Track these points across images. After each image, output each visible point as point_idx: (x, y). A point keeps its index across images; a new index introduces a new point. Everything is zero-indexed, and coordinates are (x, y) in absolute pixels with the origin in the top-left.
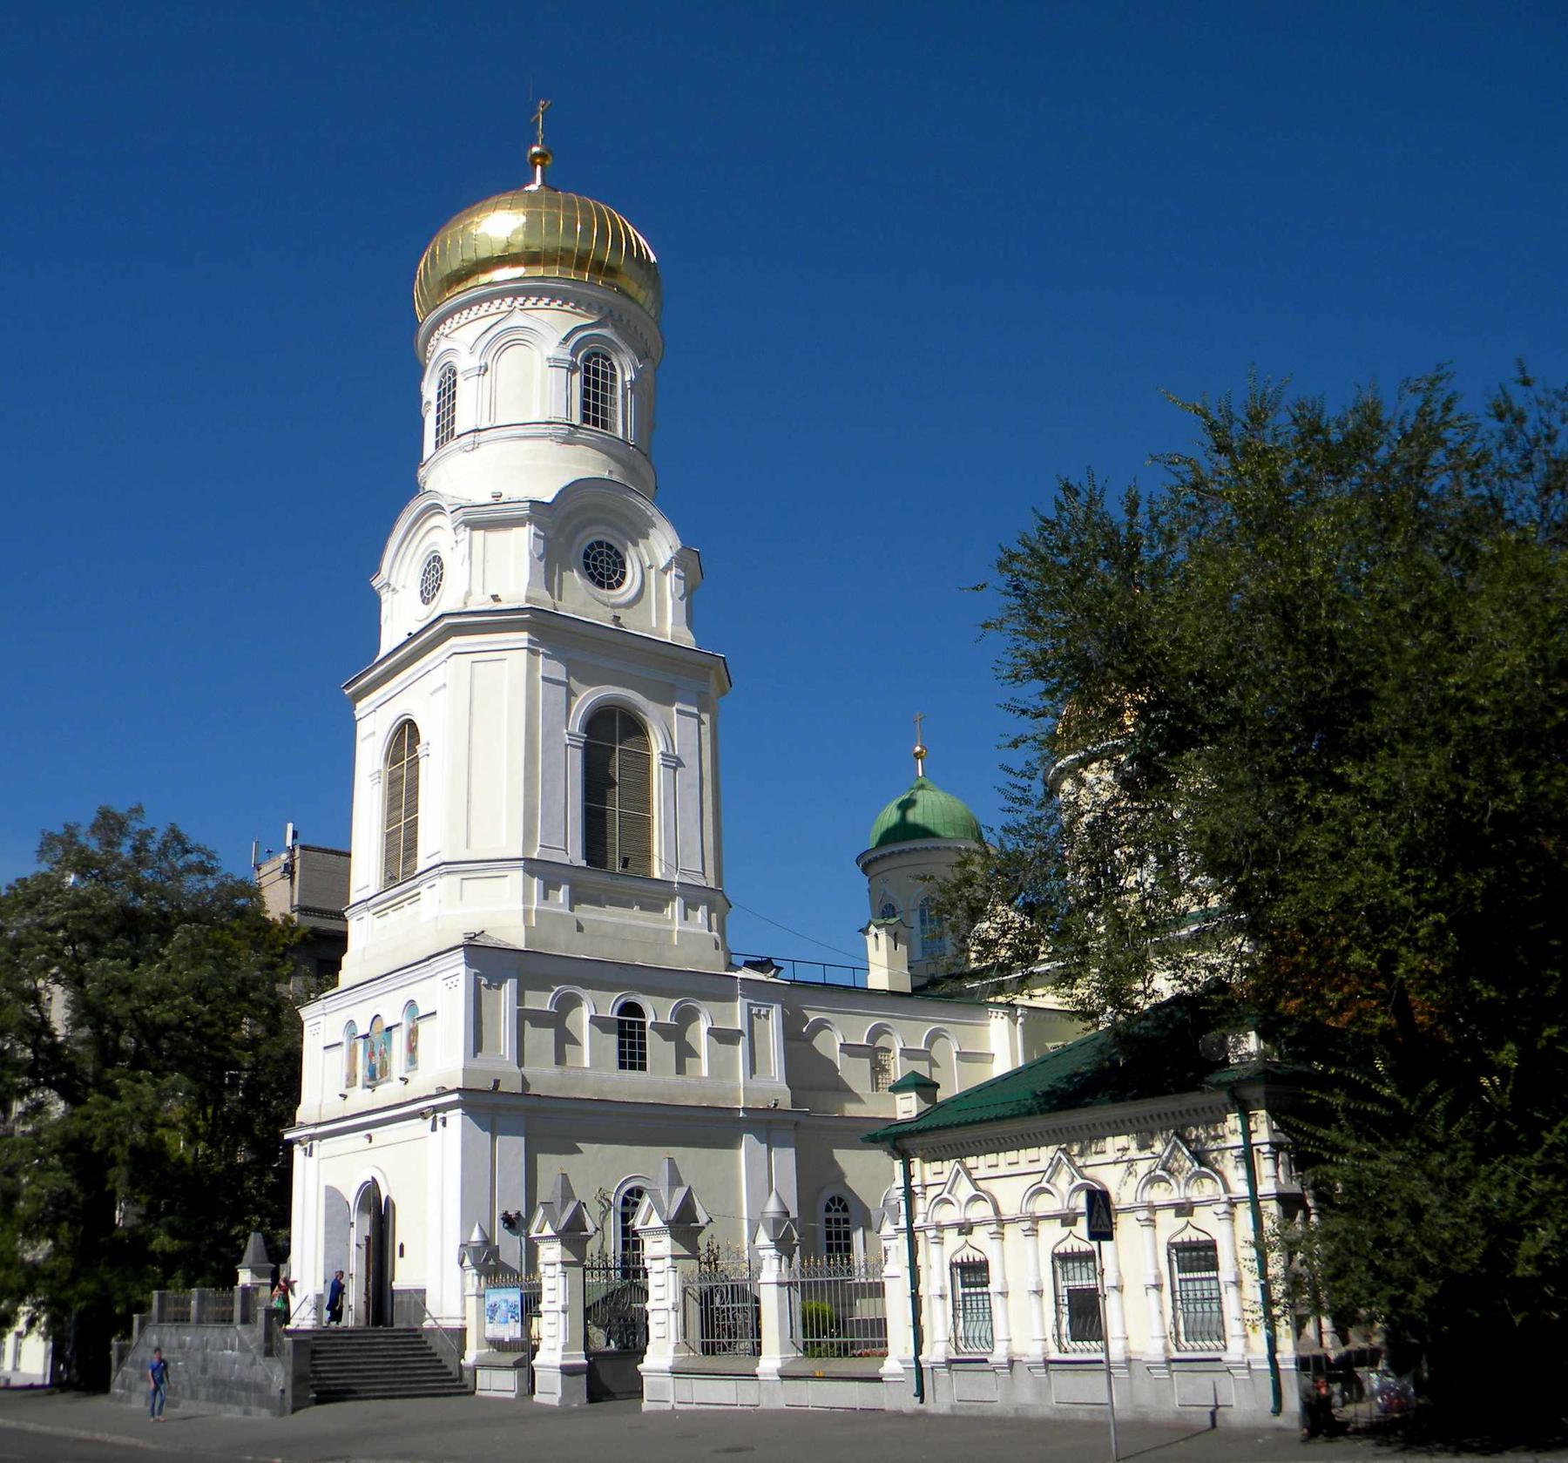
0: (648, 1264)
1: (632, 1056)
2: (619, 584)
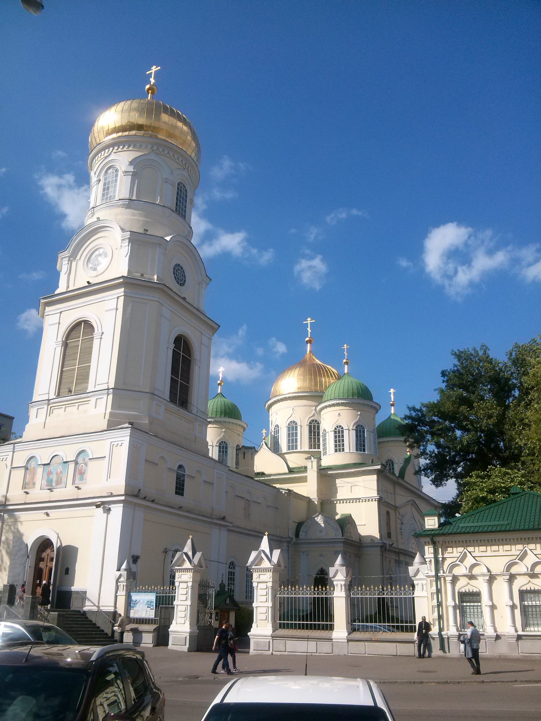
0: (255, 585)
1: (180, 490)
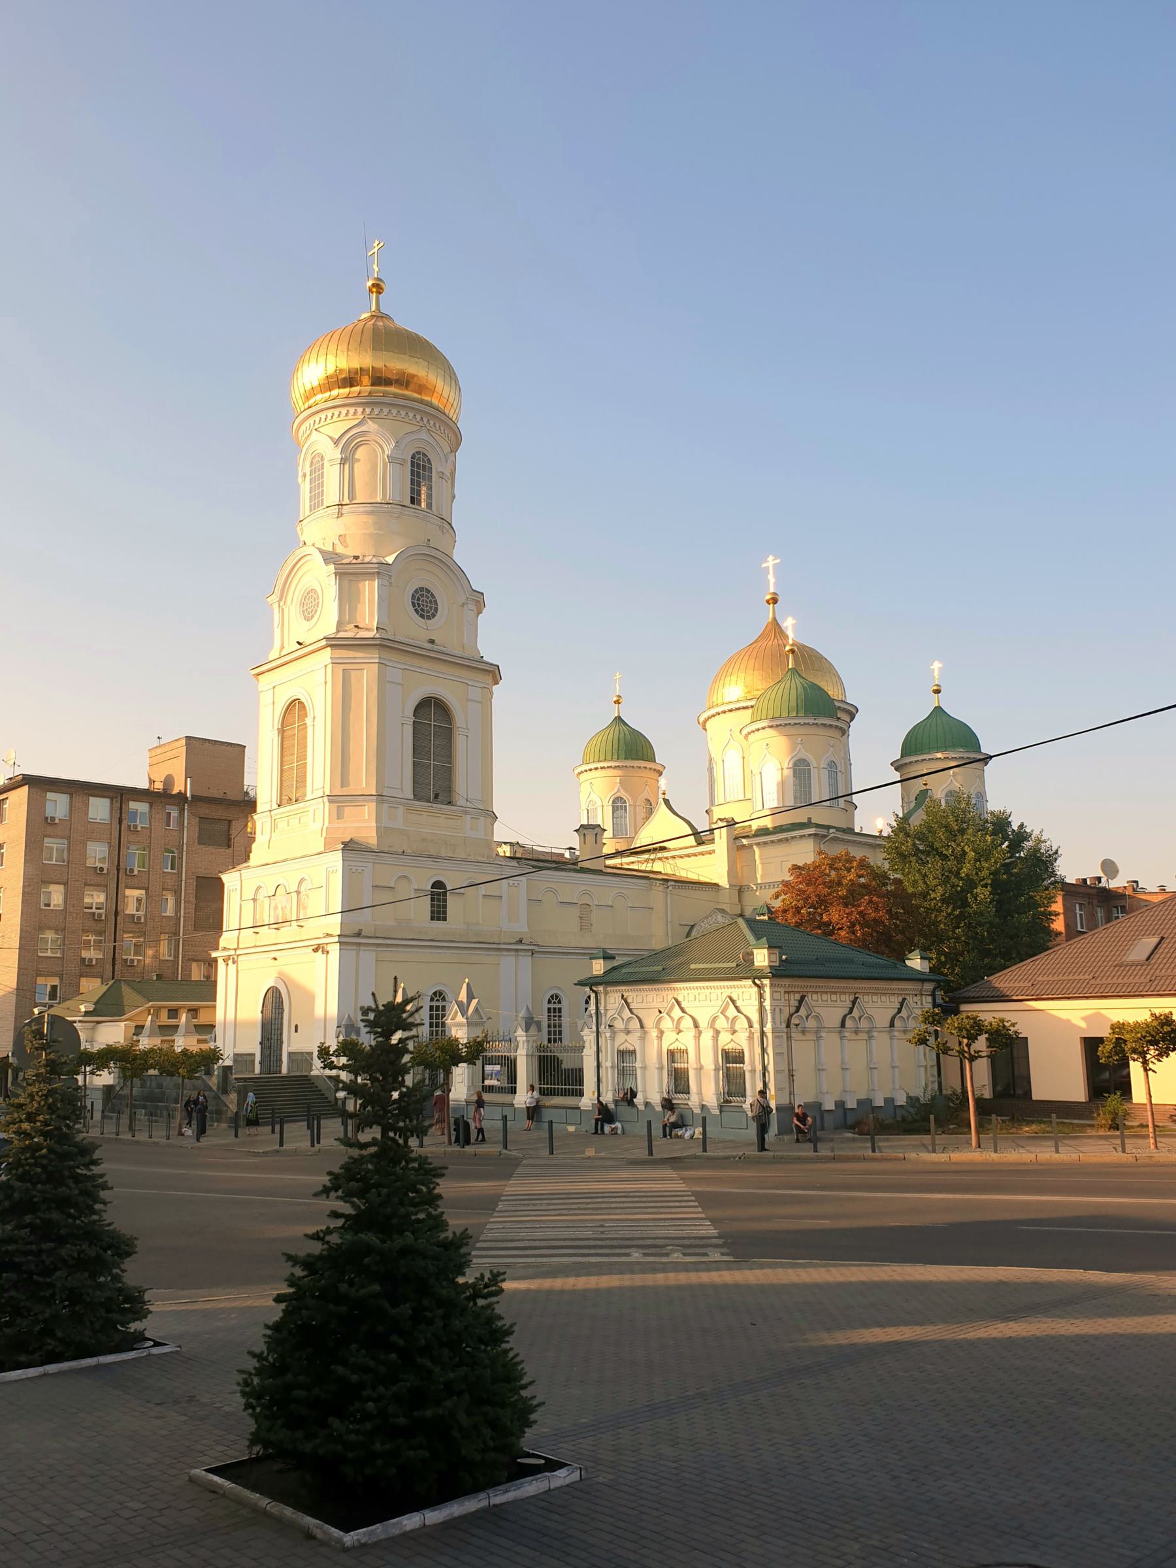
1: (439, 912)
2: (434, 616)
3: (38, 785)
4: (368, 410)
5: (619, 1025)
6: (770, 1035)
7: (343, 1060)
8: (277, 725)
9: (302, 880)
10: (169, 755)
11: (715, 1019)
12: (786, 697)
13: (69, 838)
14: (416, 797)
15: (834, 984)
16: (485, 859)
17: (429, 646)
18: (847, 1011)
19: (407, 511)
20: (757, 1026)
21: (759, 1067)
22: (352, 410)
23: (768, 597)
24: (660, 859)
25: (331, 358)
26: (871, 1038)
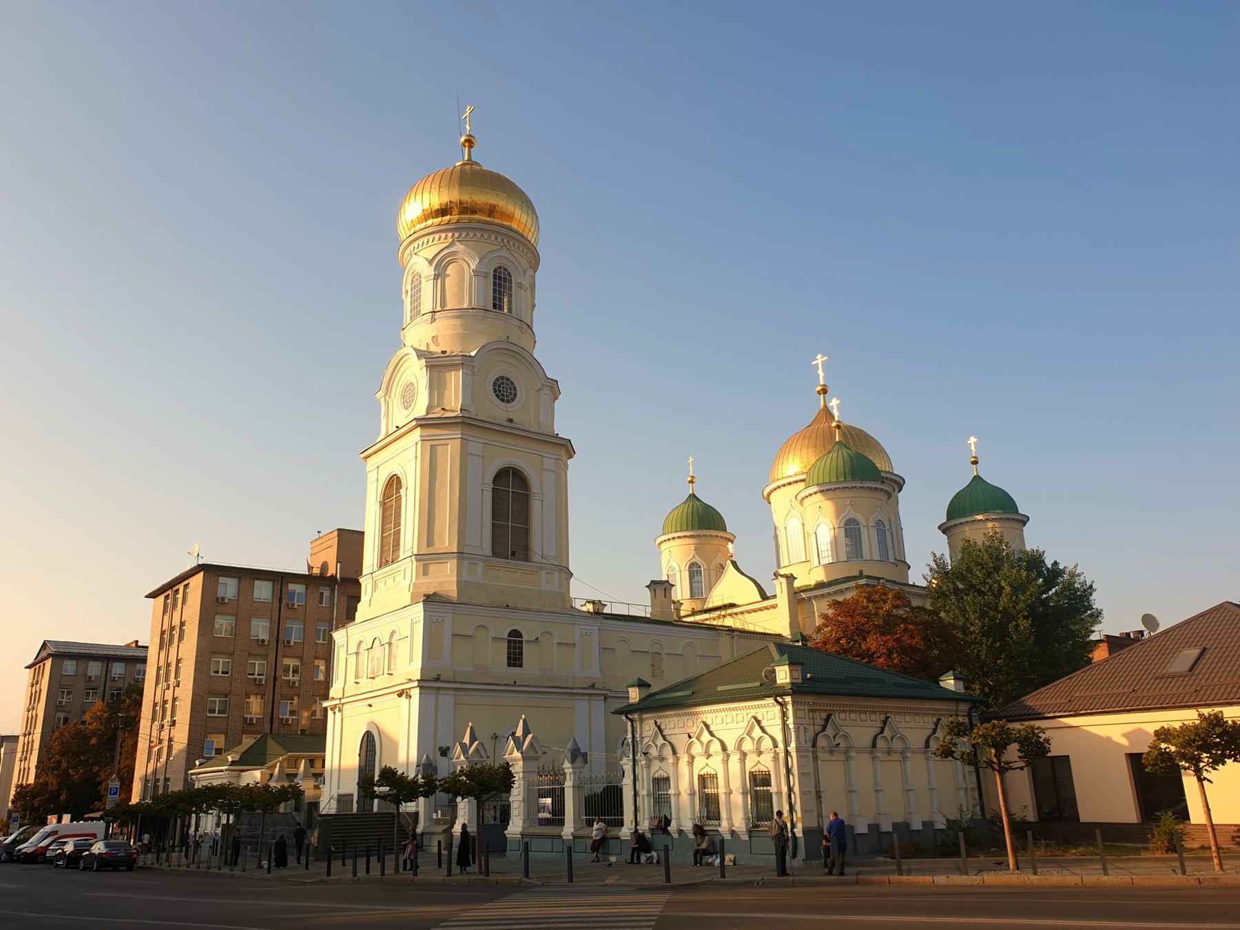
1: (515, 658)
2: (513, 400)
3: (211, 571)
4: (457, 235)
5: (654, 752)
6: (794, 754)
7: (386, 789)
8: (380, 498)
9: (393, 633)
10: (325, 545)
11: (741, 741)
12: (834, 465)
13: (236, 615)
14: (495, 553)
15: (862, 702)
16: (559, 610)
17: (508, 424)
18: (879, 730)
19: (490, 315)
20: (781, 746)
21: (785, 789)
22: (443, 235)
23: (819, 388)
24: (730, 615)
25: (426, 195)
26: (905, 758)
